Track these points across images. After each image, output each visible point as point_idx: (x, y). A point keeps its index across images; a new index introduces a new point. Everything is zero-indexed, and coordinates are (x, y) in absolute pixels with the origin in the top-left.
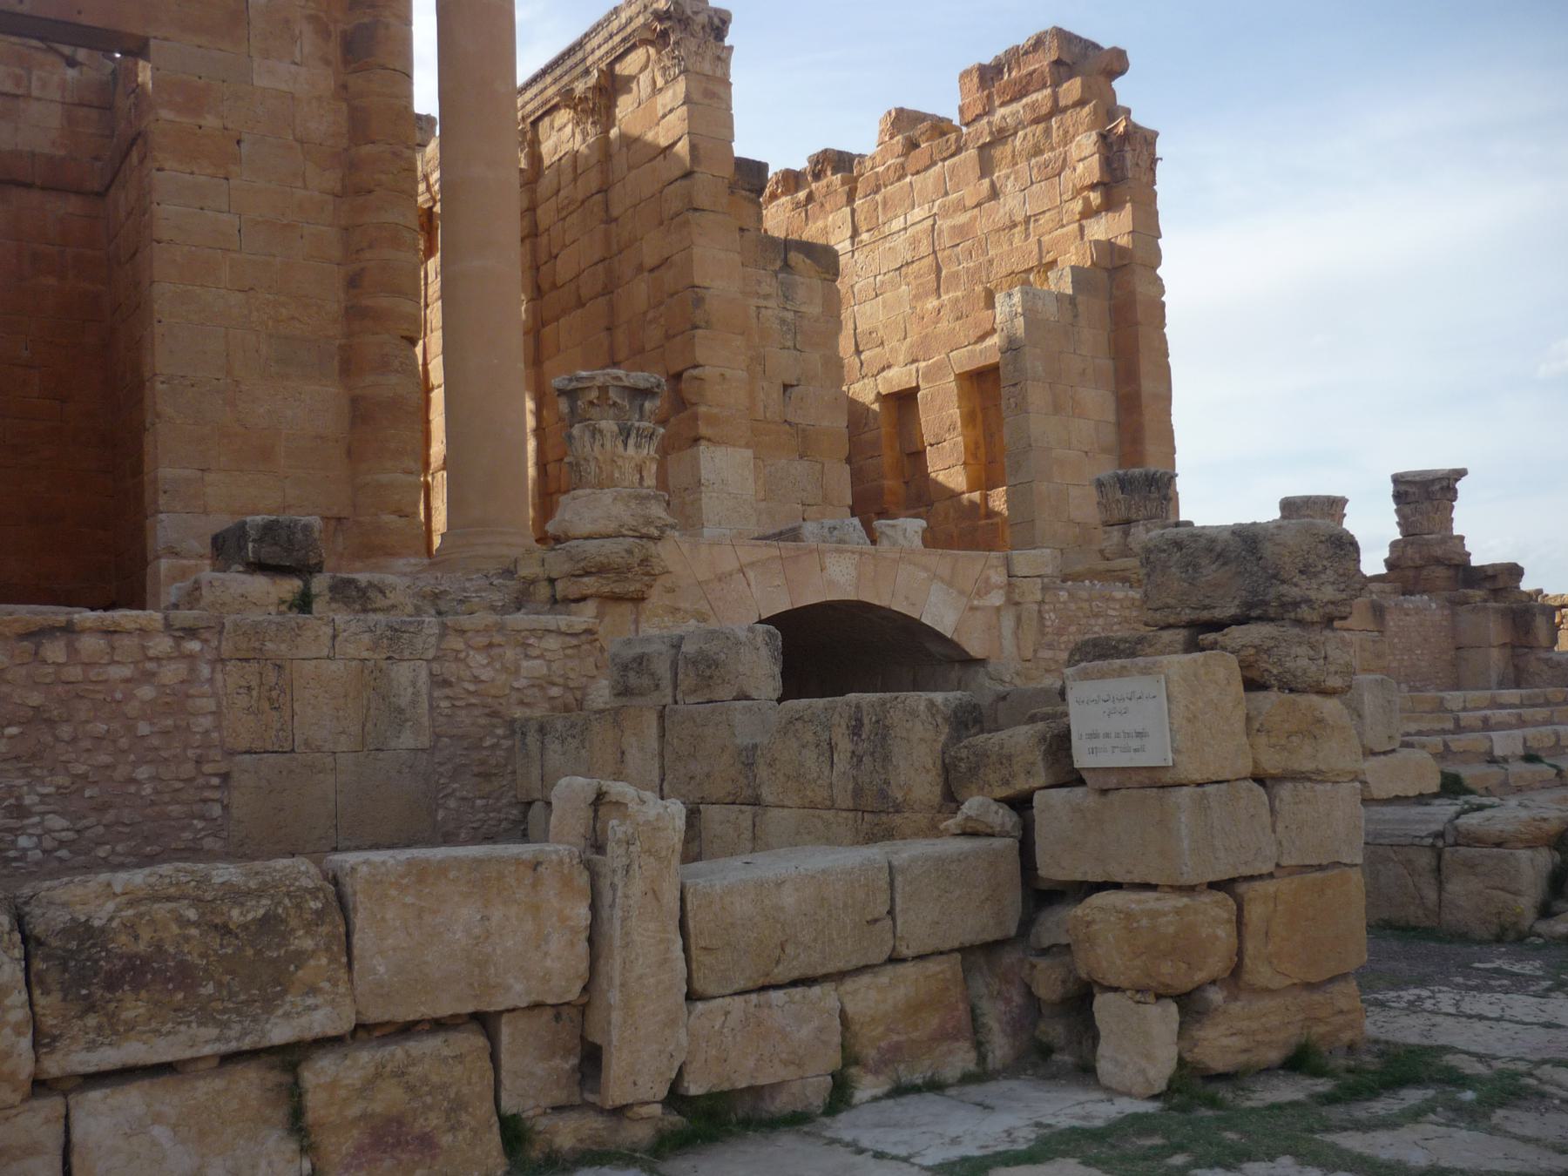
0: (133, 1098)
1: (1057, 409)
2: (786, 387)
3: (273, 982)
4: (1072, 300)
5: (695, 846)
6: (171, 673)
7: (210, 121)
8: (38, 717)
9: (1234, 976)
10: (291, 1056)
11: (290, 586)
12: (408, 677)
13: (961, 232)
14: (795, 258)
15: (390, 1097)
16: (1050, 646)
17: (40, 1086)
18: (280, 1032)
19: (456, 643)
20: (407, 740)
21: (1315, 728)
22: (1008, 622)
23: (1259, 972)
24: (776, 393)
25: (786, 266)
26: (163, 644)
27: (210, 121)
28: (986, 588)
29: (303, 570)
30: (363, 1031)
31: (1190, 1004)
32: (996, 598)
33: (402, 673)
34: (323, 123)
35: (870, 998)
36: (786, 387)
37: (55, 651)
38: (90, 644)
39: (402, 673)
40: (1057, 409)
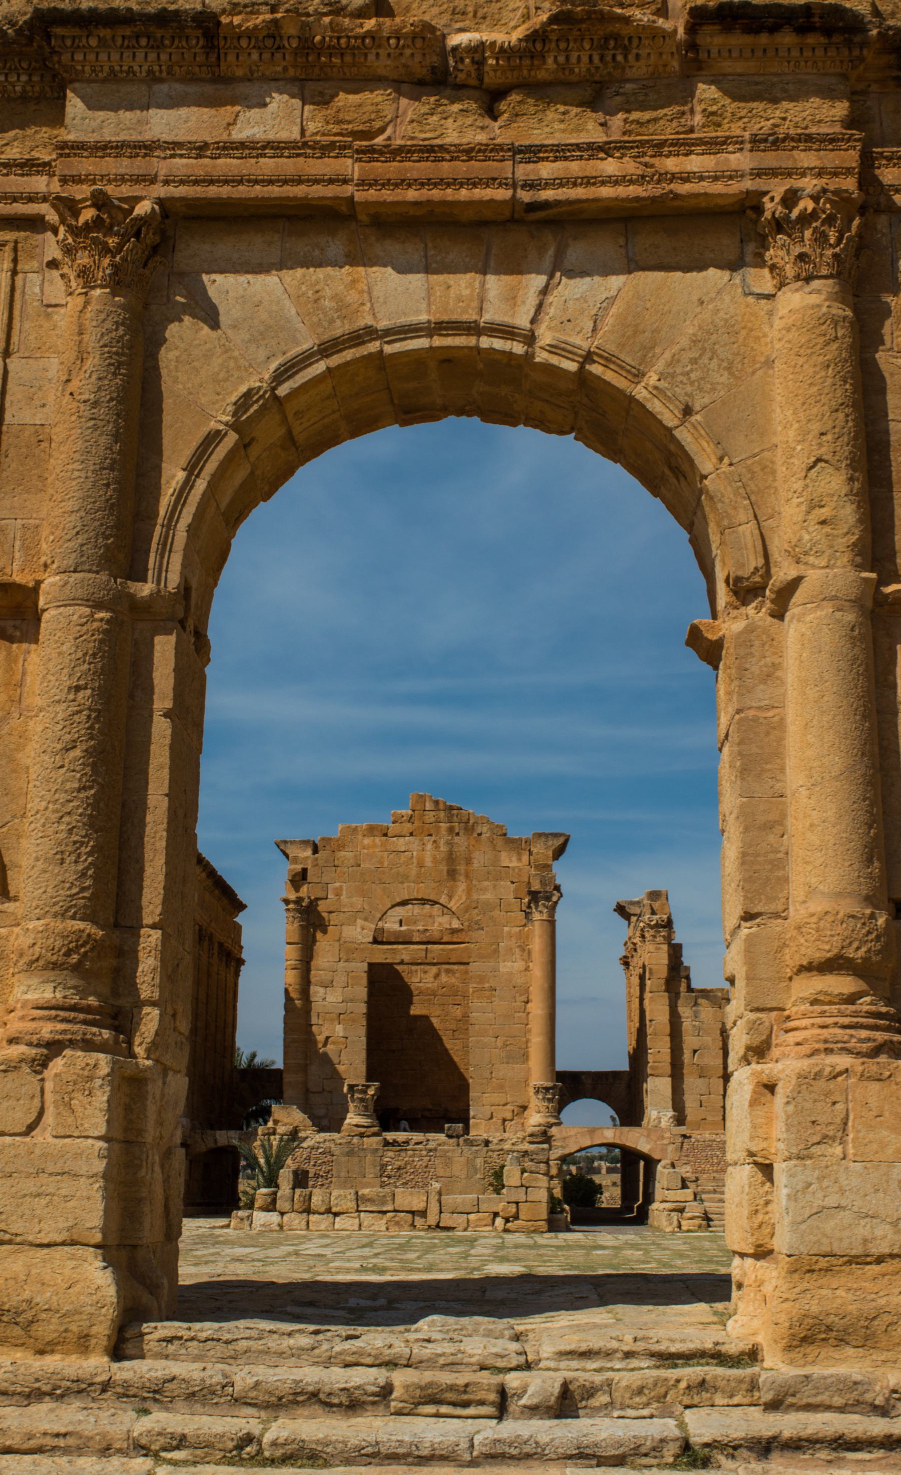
0: (368, 1214)
3: (384, 1203)
9: (516, 1217)
11: (454, 1140)
12: (479, 1162)
15: (397, 1219)
16: (687, 1156)
17: (357, 1211)
18: (384, 1209)
19: (490, 1153)
20: (478, 1176)
21: (536, 1179)
23: (521, 1217)
25: (696, 1004)
26: (424, 1153)
27: (487, 985)
28: (663, 1138)
30: (395, 1211)
31: (507, 1220)
35: (472, 1217)
37: (403, 1154)
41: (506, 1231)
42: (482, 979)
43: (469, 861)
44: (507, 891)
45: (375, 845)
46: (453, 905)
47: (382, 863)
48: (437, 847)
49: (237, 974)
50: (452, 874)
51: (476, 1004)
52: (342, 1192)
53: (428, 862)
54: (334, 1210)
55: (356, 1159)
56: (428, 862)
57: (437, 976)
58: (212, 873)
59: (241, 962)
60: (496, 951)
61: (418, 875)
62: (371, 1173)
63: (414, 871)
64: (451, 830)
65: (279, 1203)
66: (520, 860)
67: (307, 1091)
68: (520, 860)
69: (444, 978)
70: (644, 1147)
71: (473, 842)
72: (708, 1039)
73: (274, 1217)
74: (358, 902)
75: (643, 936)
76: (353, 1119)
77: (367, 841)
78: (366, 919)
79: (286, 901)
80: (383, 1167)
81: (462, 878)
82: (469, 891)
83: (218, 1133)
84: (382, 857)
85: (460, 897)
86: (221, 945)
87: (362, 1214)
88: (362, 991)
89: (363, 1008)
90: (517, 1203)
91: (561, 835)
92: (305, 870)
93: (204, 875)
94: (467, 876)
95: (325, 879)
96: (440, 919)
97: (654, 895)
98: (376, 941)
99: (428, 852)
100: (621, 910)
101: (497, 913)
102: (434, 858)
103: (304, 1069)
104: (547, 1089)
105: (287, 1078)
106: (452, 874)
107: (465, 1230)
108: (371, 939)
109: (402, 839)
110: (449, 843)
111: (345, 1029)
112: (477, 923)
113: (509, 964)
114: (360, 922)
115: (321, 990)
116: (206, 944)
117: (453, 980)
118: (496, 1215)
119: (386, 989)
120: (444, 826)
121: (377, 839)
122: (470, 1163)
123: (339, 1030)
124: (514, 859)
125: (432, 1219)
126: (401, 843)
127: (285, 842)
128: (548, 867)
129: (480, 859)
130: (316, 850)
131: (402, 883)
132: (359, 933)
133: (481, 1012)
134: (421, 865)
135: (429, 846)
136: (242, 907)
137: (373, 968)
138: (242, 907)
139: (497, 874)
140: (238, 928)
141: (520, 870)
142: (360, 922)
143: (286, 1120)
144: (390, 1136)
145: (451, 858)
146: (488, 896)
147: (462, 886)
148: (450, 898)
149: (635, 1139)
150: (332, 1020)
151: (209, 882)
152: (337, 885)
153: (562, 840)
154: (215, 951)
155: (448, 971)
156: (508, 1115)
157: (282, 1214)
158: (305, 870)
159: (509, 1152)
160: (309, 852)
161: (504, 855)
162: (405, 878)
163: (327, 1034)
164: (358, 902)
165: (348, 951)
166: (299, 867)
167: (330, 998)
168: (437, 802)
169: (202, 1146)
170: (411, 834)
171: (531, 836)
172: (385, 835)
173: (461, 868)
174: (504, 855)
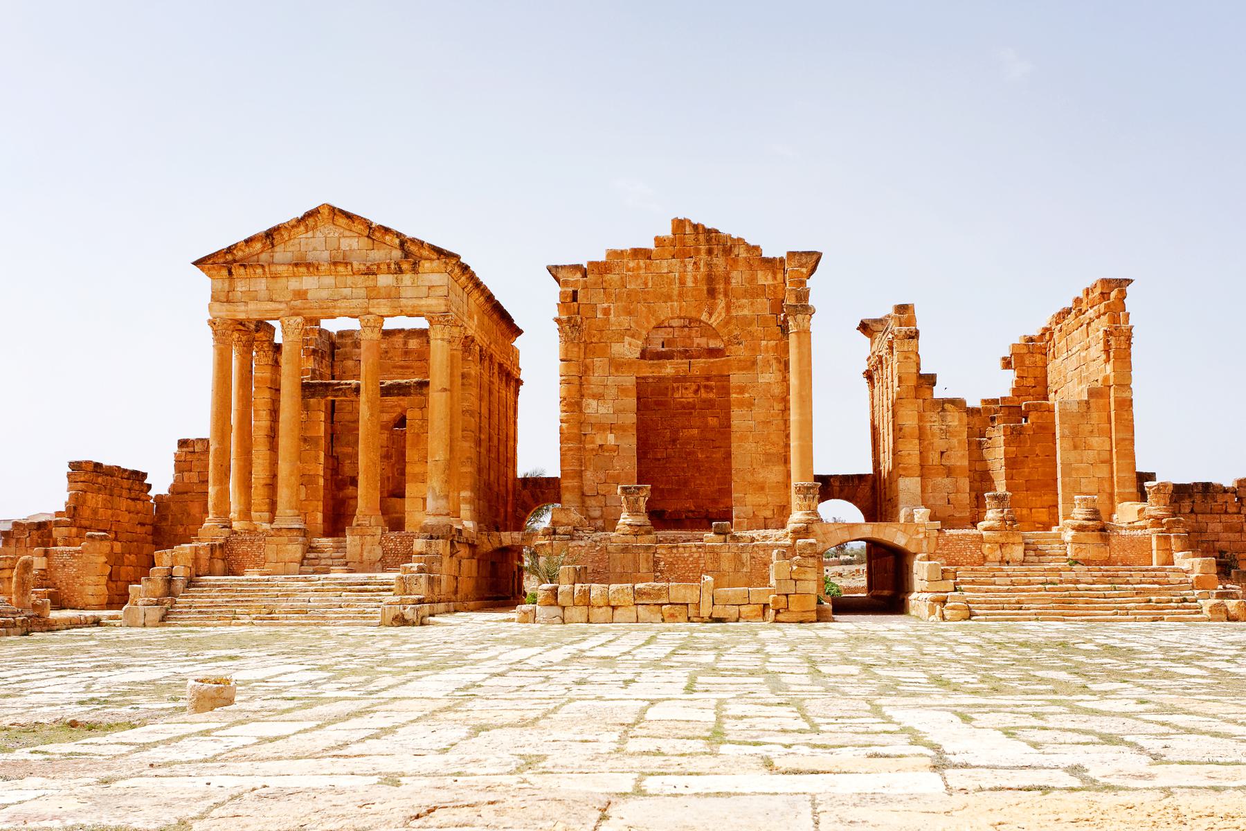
1: (1075, 447)
2: (942, 453)
3: (659, 596)
4: (1087, 402)
5: (716, 586)
6: (696, 555)
7: (747, 395)
8: (671, 563)
10: (662, 605)
13: (1085, 358)
14: (946, 406)
21: (805, 573)
22: (925, 543)
24: (937, 456)
25: (943, 410)
26: (694, 550)
28: (918, 533)
29: (725, 534)
31: (778, 612)
32: (921, 536)
33: (744, 556)
34: (777, 390)
35: (743, 608)
36: (942, 453)
37: (675, 551)
38: (681, 550)
39: (744, 556)
40: (1075, 447)
41: (776, 621)
42: (742, 390)
43: (727, 281)
44: (763, 305)
45: (639, 268)
46: (714, 321)
47: (646, 284)
48: (698, 268)
49: (517, 393)
50: (712, 293)
51: (736, 412)
52: (619, 586)
53: (690, 283)
54: (613, 603)
55: (630, 556)
56: (690, 283)
57: (696, 391)
58: (490, 297)
59: (519, 382)
60: (754, 363)
61: (680, 295)
62: (644, 567)
63: (676, 292)
64: (710, 252)
65: (560, 598)
66: (775, 278)
67: (583, 494)
68: (775, 278)
69: (703, 394)
70: (900, 540)
71: (731, 262)
72: (955, 441)
73: (556, 611)
74: (626, 321)
75: (891, 348)
76: (625, 519)
77: (631, 264)
78: (633, 336)
79: (557, 320)
80: (656, 563)
81: (721, 296)
82: (728, 308)
83: (503, 533)
84: (646, 278)
85: (720, 314)
86: (500, 365)
87: (640, 608)
88: (632, 402)
89: (631, 418)
90: (787, 595)
91: (815, 253)
92: (575, 293)
93: (482, 299)
94: (726, 295)
95: (594, 301)
96: (697, 341)
97: (902, 309)
98: (643, 355)
99: (692, 273)
100: (865, 327)
101: (754, 328)
102: (695, 278)
103: (580, 475)
104: (808, 488)
105: (565, 483)
106: (712, 293)
107: (737, 621)
108: (638, 355)
109: (664, 262)
110: (709, 265)
111: (616, 438)
112: (736, 337)
113: (767, 375)
114: (627, 339)
115: (594, 403)
116: (486, 363)
117: (711, 395)
118: (766, 606)
119: (650, 400)
120: (703, 248)
121: (642, 263)
122: (737, 558)
123: (611, 439)
124: (770, 277)
125: (705, 612)
126: (664, 266)
127: (557, 267)
128: (803, 283)
129: (737, 278)
130: (585, 275)
131: (665, 302)
132: (628, 349)
133: (740, 420)
134: (682, 283)
135: (690, 267)
136: (519, 332)
137: (641, 383)
138: (519, 332)
139: (755, 292)
140: (515, 353)
141: (775, 287)
142: (627, 339)
143: (565, 521)
144: (661, 534)
145: (710, 279)
146: (746, 312)
147: (721, 303)
148: (711, 315)
149: (892, 534)
150: (604, 430)
151: (488, 307)
152: (605, 305)
153: (815, 257)
154: (496, 370)
155: (706, 387)
156: (768, 514)
157: (564, 608)
158: (575, 293)
159: (773, 547)
160: (579, 276)
161: (760, 274)
162: (669, 298)
163: (599, 442)
164: (626, 321)
165: (618, 365)
166: (571, 290)
167: (602, 410)
168: (696, 227)
169: (488, 544)
170: (673, 257)
171: (785, 256)
172: (649, 258)
173: (720, 287)
174: (760, 274)
